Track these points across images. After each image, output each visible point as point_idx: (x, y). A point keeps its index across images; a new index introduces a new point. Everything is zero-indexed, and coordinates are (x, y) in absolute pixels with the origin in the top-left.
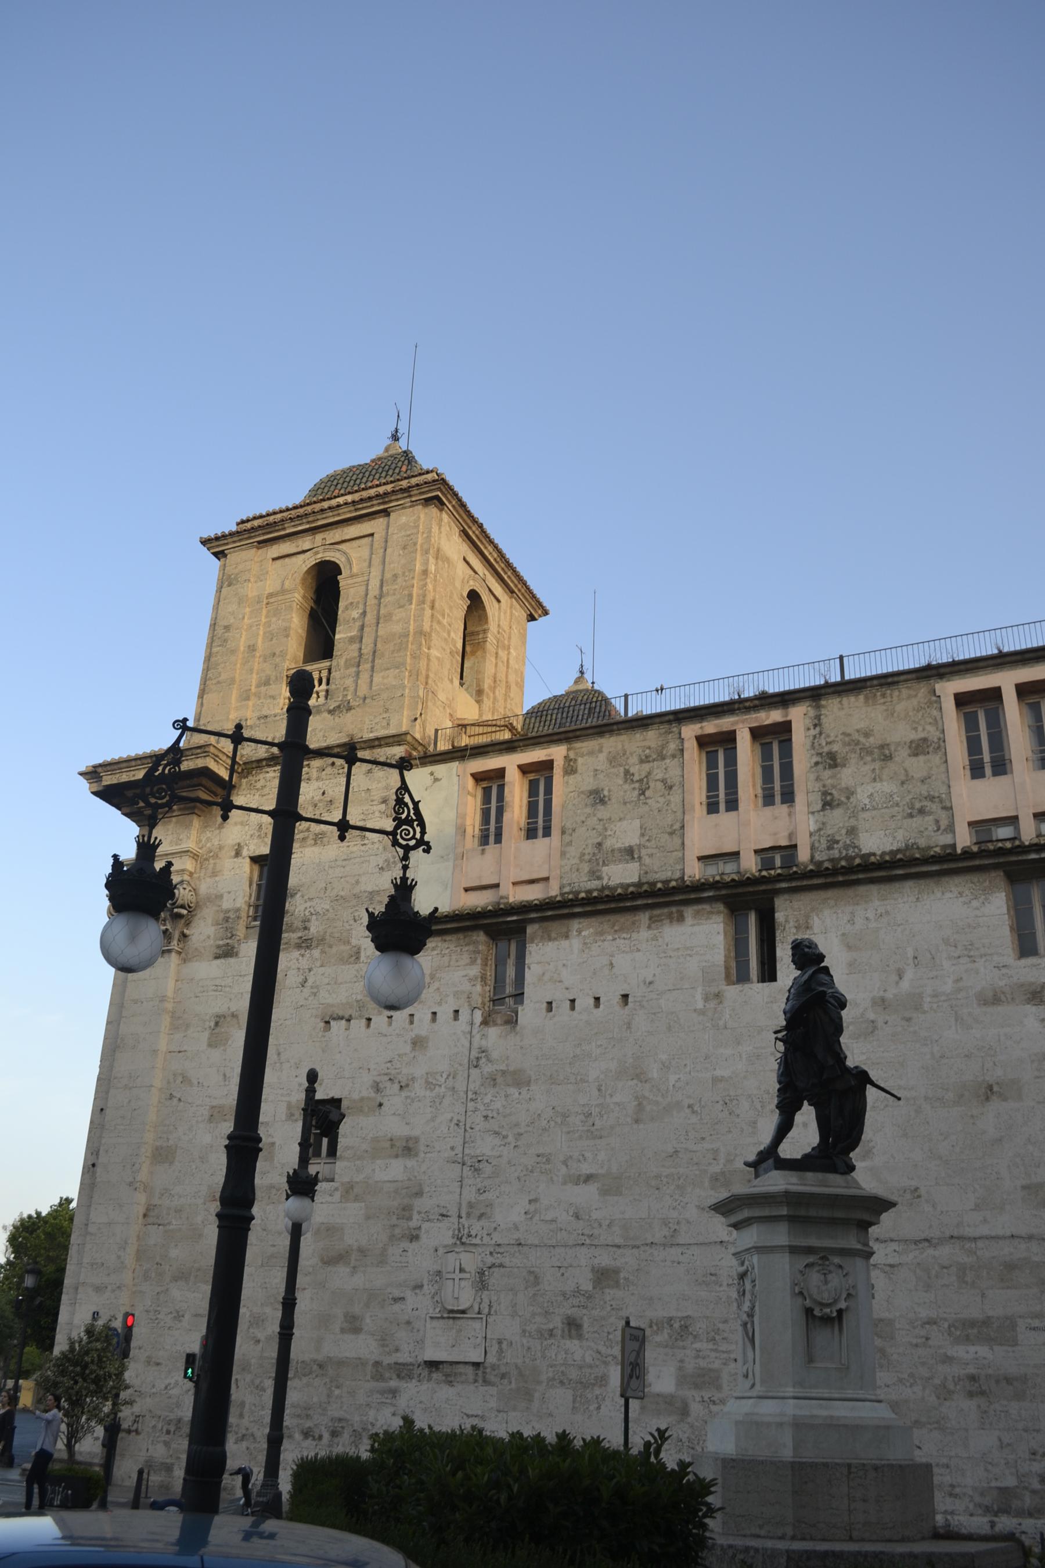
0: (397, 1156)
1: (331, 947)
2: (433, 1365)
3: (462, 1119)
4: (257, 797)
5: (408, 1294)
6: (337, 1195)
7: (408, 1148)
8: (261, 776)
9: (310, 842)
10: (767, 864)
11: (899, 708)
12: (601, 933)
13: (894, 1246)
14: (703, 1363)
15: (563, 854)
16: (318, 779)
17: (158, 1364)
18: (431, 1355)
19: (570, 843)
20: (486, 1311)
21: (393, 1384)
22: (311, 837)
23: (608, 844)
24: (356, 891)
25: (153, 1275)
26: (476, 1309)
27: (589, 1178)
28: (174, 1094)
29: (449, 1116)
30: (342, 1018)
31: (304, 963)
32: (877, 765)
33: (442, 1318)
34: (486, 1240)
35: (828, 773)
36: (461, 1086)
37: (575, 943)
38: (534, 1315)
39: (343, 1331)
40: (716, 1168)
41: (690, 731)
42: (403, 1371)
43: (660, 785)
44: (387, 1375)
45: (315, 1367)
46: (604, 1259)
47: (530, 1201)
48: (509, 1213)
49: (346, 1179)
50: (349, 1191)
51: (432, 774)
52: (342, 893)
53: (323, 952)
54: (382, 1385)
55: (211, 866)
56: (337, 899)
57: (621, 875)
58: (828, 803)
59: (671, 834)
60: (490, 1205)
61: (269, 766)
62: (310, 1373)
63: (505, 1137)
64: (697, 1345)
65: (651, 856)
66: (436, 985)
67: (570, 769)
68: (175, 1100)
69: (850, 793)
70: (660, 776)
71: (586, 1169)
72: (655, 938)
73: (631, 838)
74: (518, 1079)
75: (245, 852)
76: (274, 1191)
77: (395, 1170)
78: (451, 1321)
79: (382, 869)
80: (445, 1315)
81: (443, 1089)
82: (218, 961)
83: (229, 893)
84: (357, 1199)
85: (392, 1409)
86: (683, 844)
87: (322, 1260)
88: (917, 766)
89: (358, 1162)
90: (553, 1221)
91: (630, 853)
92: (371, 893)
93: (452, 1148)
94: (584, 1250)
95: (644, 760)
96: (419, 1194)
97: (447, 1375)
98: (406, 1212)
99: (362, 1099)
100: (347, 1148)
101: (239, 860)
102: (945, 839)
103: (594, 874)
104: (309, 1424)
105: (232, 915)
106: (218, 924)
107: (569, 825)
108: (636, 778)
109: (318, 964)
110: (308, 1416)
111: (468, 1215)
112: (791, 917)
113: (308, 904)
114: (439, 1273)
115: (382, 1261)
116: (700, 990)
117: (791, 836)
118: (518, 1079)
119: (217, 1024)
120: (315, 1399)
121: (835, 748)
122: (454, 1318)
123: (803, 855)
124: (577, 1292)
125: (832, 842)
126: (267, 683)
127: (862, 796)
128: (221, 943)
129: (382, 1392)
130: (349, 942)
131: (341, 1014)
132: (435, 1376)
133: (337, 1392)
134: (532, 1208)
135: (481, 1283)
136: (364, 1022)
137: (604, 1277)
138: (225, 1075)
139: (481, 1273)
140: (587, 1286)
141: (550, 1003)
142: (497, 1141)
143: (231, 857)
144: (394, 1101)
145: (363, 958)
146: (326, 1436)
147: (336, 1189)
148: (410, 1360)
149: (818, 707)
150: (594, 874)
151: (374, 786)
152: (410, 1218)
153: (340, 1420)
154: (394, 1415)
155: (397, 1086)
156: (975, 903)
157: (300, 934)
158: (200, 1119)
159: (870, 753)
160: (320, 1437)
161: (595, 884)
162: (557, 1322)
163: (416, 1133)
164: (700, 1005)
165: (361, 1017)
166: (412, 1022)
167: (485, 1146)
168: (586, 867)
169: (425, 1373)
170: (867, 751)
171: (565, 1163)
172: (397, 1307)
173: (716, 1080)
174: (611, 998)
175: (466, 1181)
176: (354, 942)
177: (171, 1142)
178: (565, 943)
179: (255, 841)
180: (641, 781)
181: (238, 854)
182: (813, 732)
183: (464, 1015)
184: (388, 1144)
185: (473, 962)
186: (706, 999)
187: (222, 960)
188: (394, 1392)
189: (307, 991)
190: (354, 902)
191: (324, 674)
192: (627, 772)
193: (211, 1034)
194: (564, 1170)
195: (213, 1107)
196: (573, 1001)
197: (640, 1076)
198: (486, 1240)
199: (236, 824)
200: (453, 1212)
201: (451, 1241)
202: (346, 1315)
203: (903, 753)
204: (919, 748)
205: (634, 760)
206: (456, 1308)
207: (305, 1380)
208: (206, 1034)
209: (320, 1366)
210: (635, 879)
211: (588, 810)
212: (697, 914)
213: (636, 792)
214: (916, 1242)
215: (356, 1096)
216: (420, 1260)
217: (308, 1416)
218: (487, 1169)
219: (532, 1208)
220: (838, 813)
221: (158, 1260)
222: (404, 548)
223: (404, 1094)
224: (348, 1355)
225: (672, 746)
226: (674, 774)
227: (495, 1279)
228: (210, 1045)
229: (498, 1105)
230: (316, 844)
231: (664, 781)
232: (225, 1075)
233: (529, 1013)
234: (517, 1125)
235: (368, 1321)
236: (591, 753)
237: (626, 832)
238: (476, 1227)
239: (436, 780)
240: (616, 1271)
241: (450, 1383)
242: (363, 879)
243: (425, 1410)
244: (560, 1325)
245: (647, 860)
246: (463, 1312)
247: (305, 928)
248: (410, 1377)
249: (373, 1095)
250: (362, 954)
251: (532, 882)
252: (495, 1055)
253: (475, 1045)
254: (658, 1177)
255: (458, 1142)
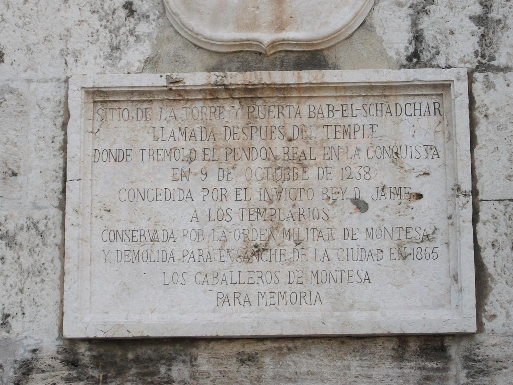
20: (464, 45)
26: (397, 38)
33: (176, 94)
78: (232, 113)
80: (196, 78)
122: (250, 94)
206: (266, 37)
246: (313, 57)
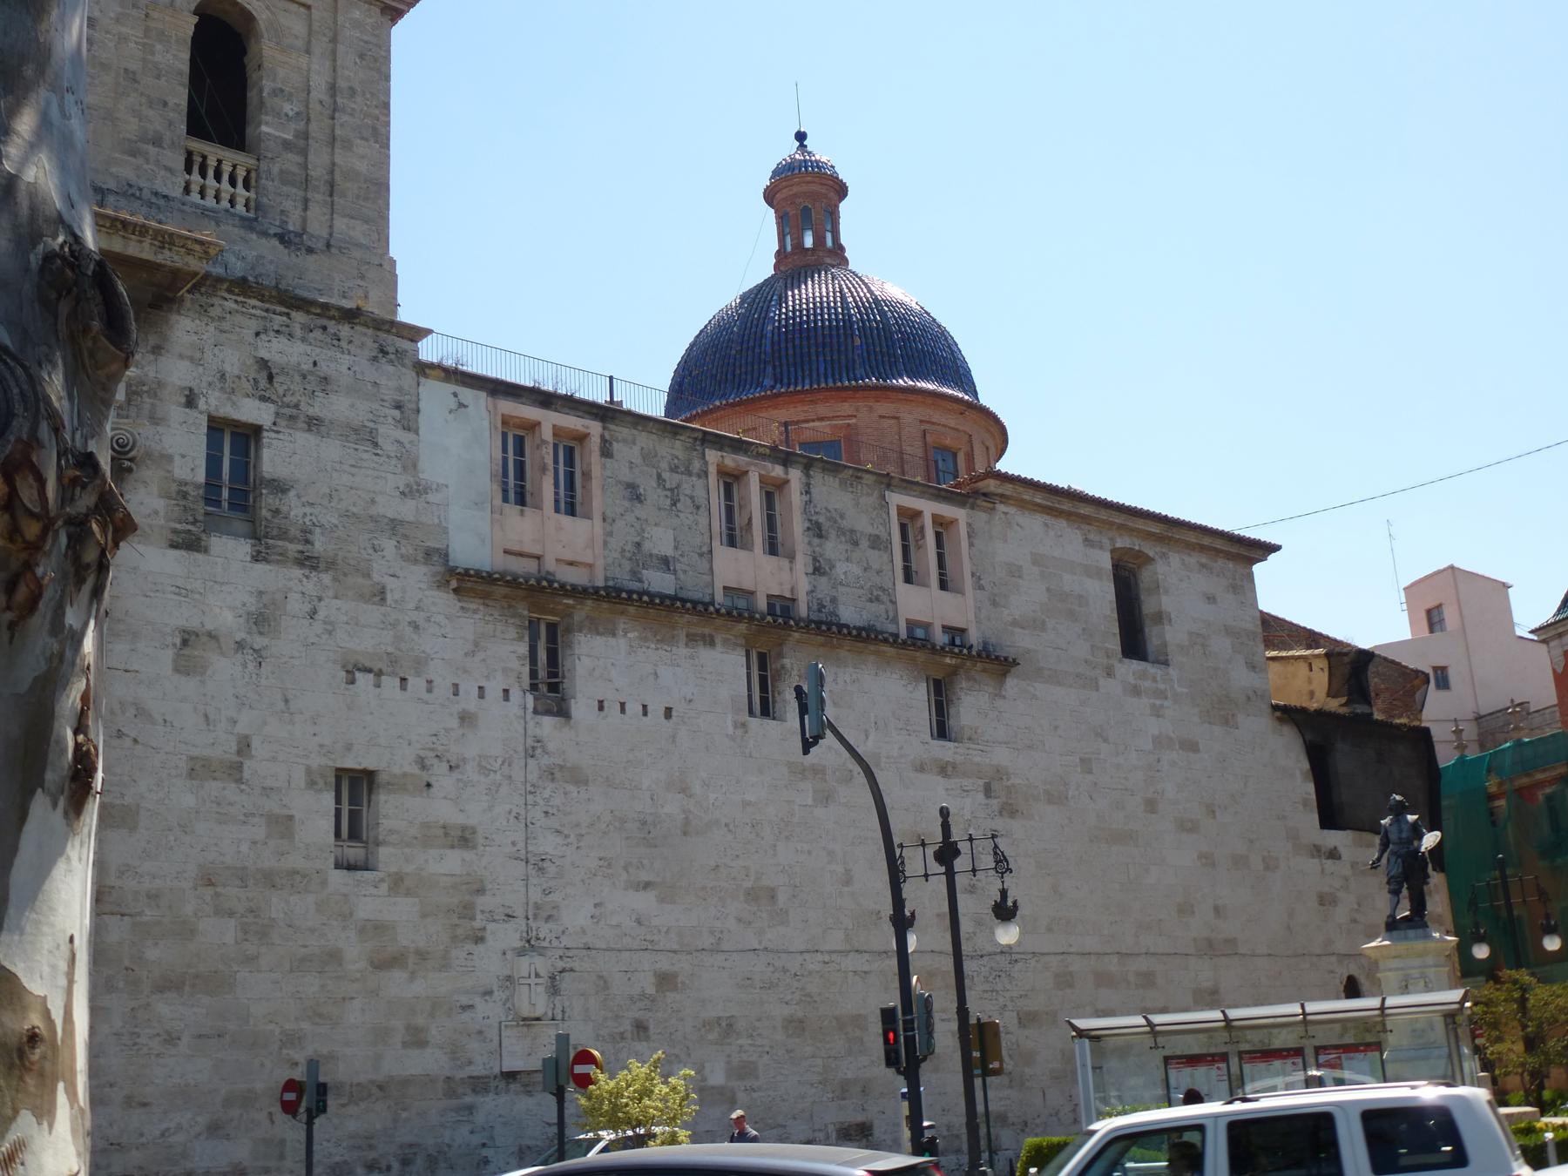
0: (452, 847)
1: (345, 575)
2: (510, 1076)
3: (523, 812)
4: (211, 328)
5: (477, 1001)
6: (384, 887)
7: (464, 839)
8: (215, 300)
9: (302, 425)
10: (771, 606)
11: (863, 500)
12: (645, 639)
13: (866, 956)
14: (745, 1057)
15: (605, 543)
16: (303, 340)
17: (145, 1105)
18: (510, 1064)
19: (610, 534)
21: (468, 1099)
22: (302, 418)
23: (647, 546)
24: (373, 511)
25: (121, 984)
27: (647, 886)
28: (125, 730)
29: (508, 807)
30: (370, 671)
31: (310, 587)
32: (849, 547)
34: (555, 943)
35: (816, 541)
36: (518, 775)
37: (620, 644)
38: (606, 1019)
39: (405, 1045)
40: (748, 884)
41: (712, 456)
42: (479, 1085)
43: (689, 501)
44: (461, 1090)
45: (374, 1090)
46: (664, 964)
47: (596, 905)
48: (576, 916)
49: (393, 869)
50: (397, 883)
51: (455, 395)
52: (355, 510)
53: (335, 579)
54: (454, 1102)
55: (147, 406)
56: (347, 515)
57: (659, 582)
58: (817, 570)
59: (701, 555)
60: (556, 907)
61: (229, 291)
62: (370, 1095)
63: (567, 836)
64: (740, 1042)
65: (685, 572)
66: (481, 655)
67: (606, 452)
68: (128, 742)
69: (832, 567)
70: (688, 492)
71: (644, 876)
72: (692, 657)
73: (666, 549)
74: (577, 778)
75: (202, 404)
76: (298, 878)
77: (452, 862)
79: (403, 493)
81: (498, 777)
82: (177, 553)
83: (183, 456)
84: (408, 893)
85: (469, 1127)
86: (711, 569)
87: (372, 963)
88: (873, 555)
89: (407, 850)
90: (618, 926)
91: (666, 563)
92: (393, 520)
93: (514, 844)
94: (646, 954)
95: (674, 469)
96: (481, 891)
97: (525, 1086)
98: (467, 911)
99: (405, 775)
100: (391, 832)
101: (193, 413)
102: (891, 628)
103: (635, 575)
104: (372, 1155)
105: (189, 489)
106: (170, 498)
107: (608, 513)
108: (668, 485)
109: (331, 593)
110: (371, 1147)
111: (535, 916)
112: (795, 664)
113: (308, 510)
114: (509, 978)
115: (445, 966)
116: (730, 717)
117: (792, 589)
118: (577, 778)
119: (185, 642)
120: (378, 1126)
121: (821, 519)
123: (803, 610)
124: (643, 995)
125: (821, 606)
126: (157, 141)
127: (841, 569)
128: (178, 526)
129: (457, 1110)
130: (368, 576)
131: (368, 664)
132: (513, 1087)
133: (404, 1115)
134: (597, 912)
135: (554, 990)
136: (398, 681)
137: (665, 981)
138: (206, 716)
139: (552, 978)
140: (651, 990)
141: (601, 703)
142: (560, 840)
143: (179, 405)
144: (444, 782)
145: (389, 601)
146: (396, 1165)
147: (382, 880)
148: (484, 1073)
149: (808, 476)
150: (635, 575)
151: (383, 381)
152: (473, 918)
153: (411, 1145)
154: (472, 1132)
155: (445, 766)
156: (910, 688)
157: (300, 547)
158: (173, 772)
159: (844, 534)
160: (389, 1168)
161: (635, 585)
162: (627, 1026)
163: (472, 822)
164: (730, 730)
165: (393, 674)
166: (456, 694)
167: (548, 844)
168: (627, 566)
169: (502, 1085)
170: (841, 531)
171: (625, 868)
172: (466, 1016)
173: (746, 804)
174: (656, 710)
175: (533, 881)
176: (376, 577)
177: (128, 800)
178: (612, 641)
179: (217, 394)
180: (671, 490)
181: (191, 401)
182: (806, 498)
183: (515, 695)
184: (440, 832)
185: (520, 639)
186: (735, 727)
187: (183, 553)
188: (470, 1109)
189: (318, 627)
190: (371, 525)
191: (241, 174)
192: (659, 476)
193: (178, 655)
194: (624, 876)
195: (192, 758)
196: (623, 705)
197: (685, 790)
198: (555, 943)
199: (181, 356)
200: (520, 912)
201: (519, 944)
202: (408, 1027)
203: (864, 543)
204: (877, 543)
205: (664, 465)
207: (363, 1105)
208: (169, 654)
209: (381, 1088)
210: (671, 592)
211: (627, 504)
212: (725, 641)
213: (668, 502)
214: (880, 953)
215: (396, 770)
216: (488, 963)
217: (371, 1147)
218: (551, 869)
219: (597, 912)
220: (824, 580)
221: (127, 963)
222: (362, 56)
223: (456, 775)
224: (413, 1072)
225: (696, 465)
226: (700, 493)
227: (566, 983)
228: (177, 670)
229: (558, 800)
230: (309, 430)
231: (692, 498)
232: (206, 716)
233: (581, 708)
234: (578, 825)
235: (434, 1032)
236: (625, 441)
237: (661, 541)
238: (544, 930)
239: (462, 405)
240: (674, 976)
241: (529, 1093)
242: (379, 499)
243: (505, 1124)
244: (629, 1028)
245: (682, 576)
246: (538, 1019)
247: (307, 542)
248: (486, 1091)
249: (416, 770)
250: (389, 596)
251: (571, 563)
252: (551, 747)
253: (529, 732)
254: (704, 888)
255: (519, 837)
